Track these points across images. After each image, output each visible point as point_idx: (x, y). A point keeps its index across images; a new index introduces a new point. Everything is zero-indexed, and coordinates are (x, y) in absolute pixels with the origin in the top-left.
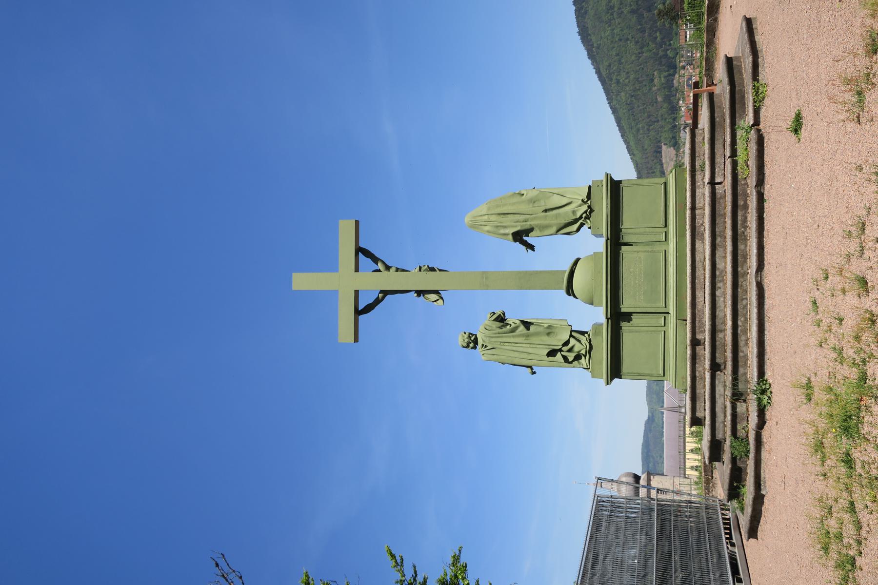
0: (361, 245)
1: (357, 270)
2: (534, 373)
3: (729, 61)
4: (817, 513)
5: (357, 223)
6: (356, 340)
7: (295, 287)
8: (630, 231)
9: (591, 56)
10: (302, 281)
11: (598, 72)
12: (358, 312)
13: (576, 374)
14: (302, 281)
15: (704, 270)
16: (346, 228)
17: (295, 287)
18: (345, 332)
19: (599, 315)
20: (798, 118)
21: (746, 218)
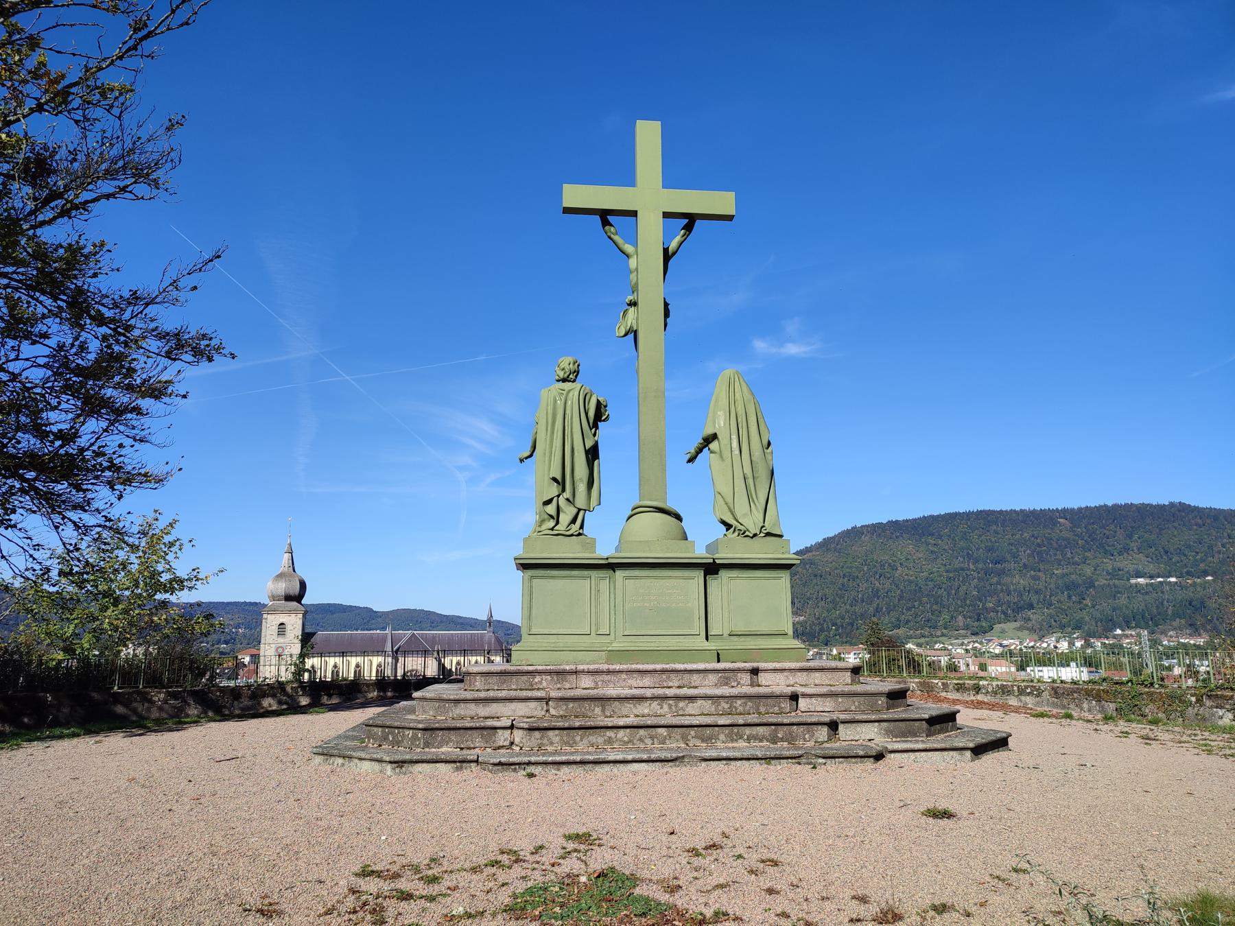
0: (698, 223)
1: (666, 215)
2: (521, 461)
3: (950, 718)
4: (421, 859)
5: (729, 218)
6: (567, 211)
7: (640, 124)
8: (725, 588)
10: (648, 137)
12: (605, 215)
13: (529, 517)
14: (648, 137)
15: (679, 687)
16: (722, 202)
17: (640, 124)
18: (576, 195)
19: (605, 550)
20: (947, 814)
21: (761, 741)
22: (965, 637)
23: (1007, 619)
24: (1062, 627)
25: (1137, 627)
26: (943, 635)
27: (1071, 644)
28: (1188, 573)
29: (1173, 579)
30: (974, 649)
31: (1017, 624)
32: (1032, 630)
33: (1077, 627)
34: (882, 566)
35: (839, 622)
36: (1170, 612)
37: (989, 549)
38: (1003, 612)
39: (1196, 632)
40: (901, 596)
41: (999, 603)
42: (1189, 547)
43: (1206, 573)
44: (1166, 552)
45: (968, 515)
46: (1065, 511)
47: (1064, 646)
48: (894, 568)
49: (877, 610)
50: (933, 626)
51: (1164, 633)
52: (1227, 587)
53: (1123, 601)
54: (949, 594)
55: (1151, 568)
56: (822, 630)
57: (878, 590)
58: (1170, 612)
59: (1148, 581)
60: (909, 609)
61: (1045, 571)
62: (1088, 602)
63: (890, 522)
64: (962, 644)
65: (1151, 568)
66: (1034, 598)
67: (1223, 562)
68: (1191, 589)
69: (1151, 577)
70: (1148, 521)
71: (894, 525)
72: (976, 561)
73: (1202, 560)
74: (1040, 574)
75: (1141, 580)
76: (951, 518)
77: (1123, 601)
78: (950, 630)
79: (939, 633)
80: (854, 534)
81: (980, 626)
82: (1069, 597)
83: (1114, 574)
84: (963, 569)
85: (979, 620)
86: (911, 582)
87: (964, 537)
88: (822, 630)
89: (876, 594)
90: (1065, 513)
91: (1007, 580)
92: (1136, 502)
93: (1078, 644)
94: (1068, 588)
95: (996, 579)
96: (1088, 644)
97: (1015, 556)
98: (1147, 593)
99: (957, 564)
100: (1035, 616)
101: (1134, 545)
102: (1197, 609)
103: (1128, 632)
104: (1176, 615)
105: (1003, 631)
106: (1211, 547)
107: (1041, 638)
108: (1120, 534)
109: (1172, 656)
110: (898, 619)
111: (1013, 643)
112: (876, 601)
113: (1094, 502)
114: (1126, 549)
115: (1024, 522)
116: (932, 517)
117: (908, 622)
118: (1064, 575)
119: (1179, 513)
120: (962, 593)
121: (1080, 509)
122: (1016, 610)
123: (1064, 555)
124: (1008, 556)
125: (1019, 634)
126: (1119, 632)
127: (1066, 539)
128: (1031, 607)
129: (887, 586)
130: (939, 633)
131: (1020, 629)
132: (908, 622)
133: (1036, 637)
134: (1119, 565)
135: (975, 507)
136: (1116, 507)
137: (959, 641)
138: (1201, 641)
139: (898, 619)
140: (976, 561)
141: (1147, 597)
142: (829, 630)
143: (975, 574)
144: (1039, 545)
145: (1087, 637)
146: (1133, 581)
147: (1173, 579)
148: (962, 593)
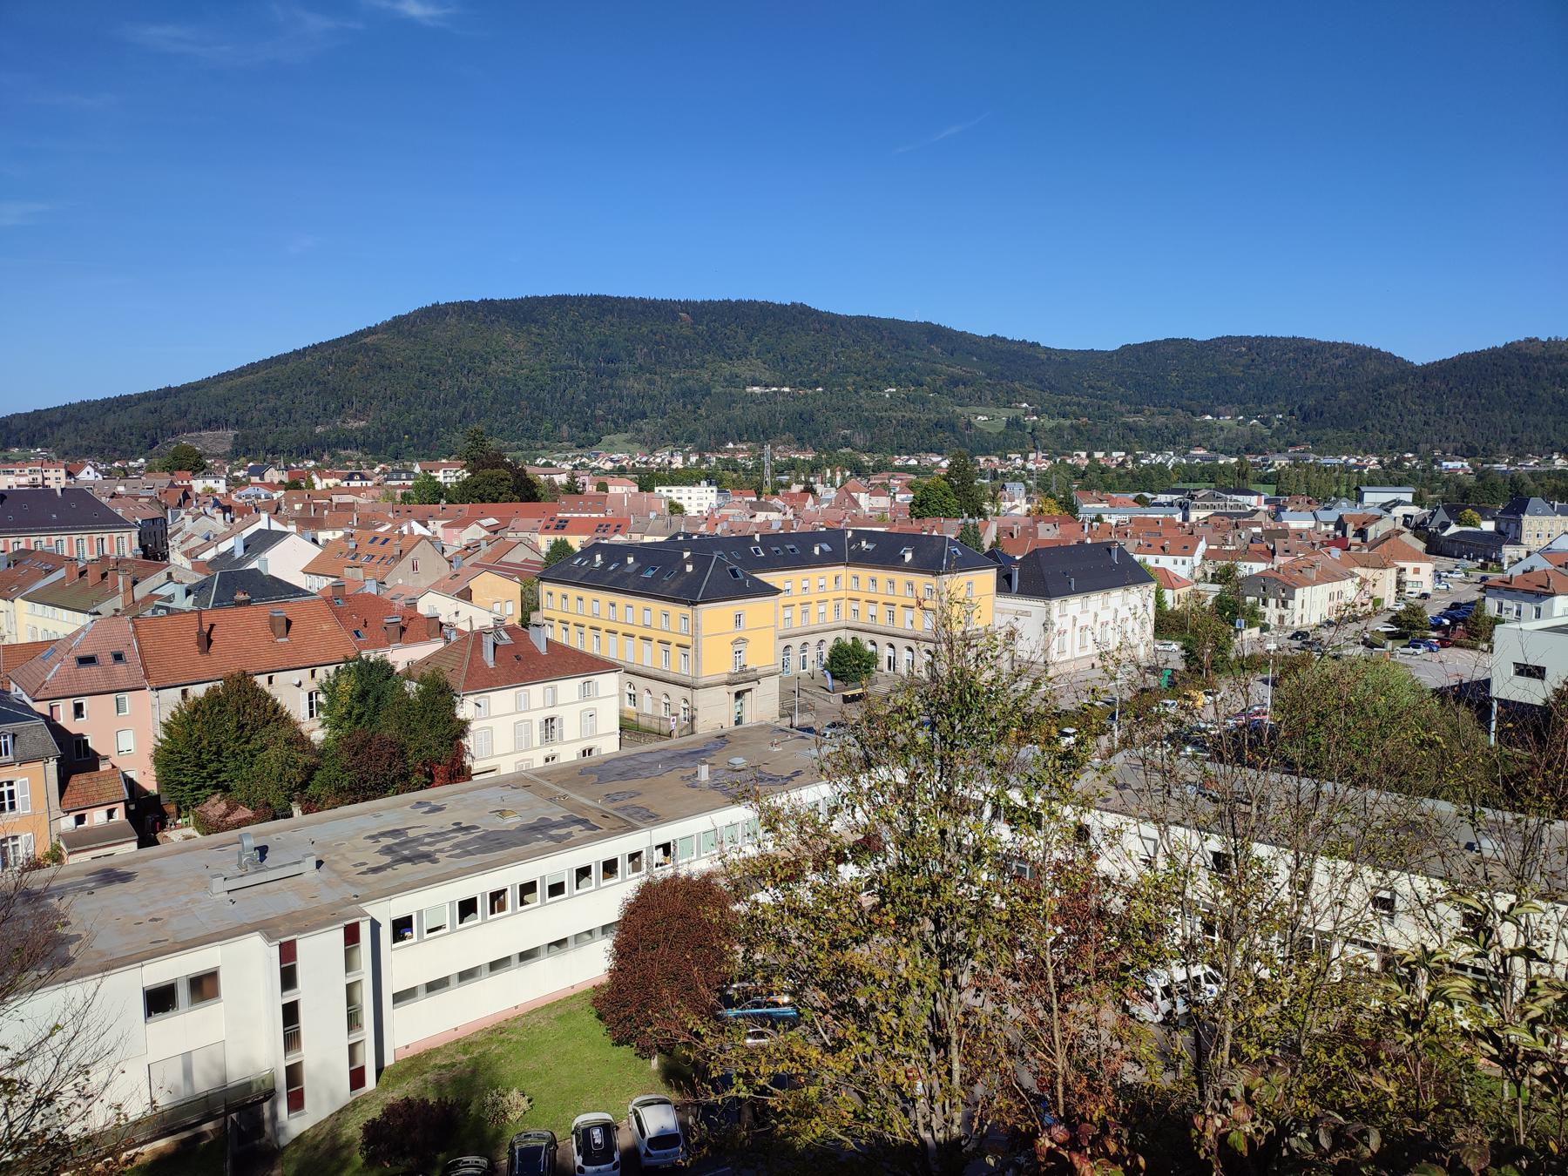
9: (398, 322)
11: (371, 331)
22: (569, 450)
23: (617, 429)
24: (675, 439)
25: (749, 440)
26: (544, 448)
27: (686, 459)
28: (801, 383)
29: (787, 389)
30: (582, 464)
31: (628, 436)
32: (643, 443)
33: (690, 440)
34: (472, 359)
35: (413, 429)
37: (603, 344)
38: (614, 422)
39: (802, 448)
40: (495, 400)
41: (610, 411)
42: (805, 354)
43: (817, 384)
45: (580, 300)
46: (687, 303)
47: (678, 462)
48: (487, 362)
49: (465, 415)
50: (537, 436)
53: (737, 412)
54: (553, 398)
56: (390, 439)
57: (466, 390)
60: (504, 415)
61: (662, 374)
62: (703, 411)
63: (484, 302)
64: (566, 459)
65: (766, 376)
66: (648, 406)
69: (767, 386)
70: (769, 322)
71: (489, 306)
72: (587, 359)
73: (816, 370)
74: (657, 378)
75: (756, 389)
76: (560, 303)
77: (737, 412)
78: (551, 441)
79: (539, 445)
80: (435, 313)
81: (587, 444)
82: (685, 406)
83: (732, 380)
84: (570, 367)
85: (586, 430)
86: (507, 380)
87: (573, 329)
88: (390, 439)
89: (463, 394)
90: (687, 306)
91: (620, 382)
92: (760, 299)
93: (693, 459)
94: (684, 395)
95: (607, 382)
96: (702, 460)
97: (631, 355)
99: (564, 361)
100: (647, 426)
101: (753, 350)
102: (806, 422)
104: (787, 428)
105: (612, 444)
106: (824, 355)
107: (652, 452)
108: (741, 334)
109: (781, 473)
110: (490, 428)
111: (624, 459)
112: (463, 404)
113: (717, 297)
114: (745, 353)
115: (643, 313)
116: (536, 298)
117: (502, 430)
118: (681, 380)
119: (799, 315)
120: (568, 396)
121: (703, 302)
122: (627, 419)
123: (682, 355)
124: (623, 354)
125: (629, 446)
126: (731, 445)
127: (686, 338)
128: (644, 415)
129: (478, 385)
130: (539, 445)
131: (629, 441)
132: (502, 430)
133: (647, 451)
135: (587, 292)
136: (739, 302)
137: (562, 455)
138: (810, 456)
139: (490, 428)
140: (587, 359)
142: (400, 439)
143: (585, 375)
144: (657, 343)
145: (700, 451)
146: (749, 390)
147: (787, 389)
148: (568, 396)
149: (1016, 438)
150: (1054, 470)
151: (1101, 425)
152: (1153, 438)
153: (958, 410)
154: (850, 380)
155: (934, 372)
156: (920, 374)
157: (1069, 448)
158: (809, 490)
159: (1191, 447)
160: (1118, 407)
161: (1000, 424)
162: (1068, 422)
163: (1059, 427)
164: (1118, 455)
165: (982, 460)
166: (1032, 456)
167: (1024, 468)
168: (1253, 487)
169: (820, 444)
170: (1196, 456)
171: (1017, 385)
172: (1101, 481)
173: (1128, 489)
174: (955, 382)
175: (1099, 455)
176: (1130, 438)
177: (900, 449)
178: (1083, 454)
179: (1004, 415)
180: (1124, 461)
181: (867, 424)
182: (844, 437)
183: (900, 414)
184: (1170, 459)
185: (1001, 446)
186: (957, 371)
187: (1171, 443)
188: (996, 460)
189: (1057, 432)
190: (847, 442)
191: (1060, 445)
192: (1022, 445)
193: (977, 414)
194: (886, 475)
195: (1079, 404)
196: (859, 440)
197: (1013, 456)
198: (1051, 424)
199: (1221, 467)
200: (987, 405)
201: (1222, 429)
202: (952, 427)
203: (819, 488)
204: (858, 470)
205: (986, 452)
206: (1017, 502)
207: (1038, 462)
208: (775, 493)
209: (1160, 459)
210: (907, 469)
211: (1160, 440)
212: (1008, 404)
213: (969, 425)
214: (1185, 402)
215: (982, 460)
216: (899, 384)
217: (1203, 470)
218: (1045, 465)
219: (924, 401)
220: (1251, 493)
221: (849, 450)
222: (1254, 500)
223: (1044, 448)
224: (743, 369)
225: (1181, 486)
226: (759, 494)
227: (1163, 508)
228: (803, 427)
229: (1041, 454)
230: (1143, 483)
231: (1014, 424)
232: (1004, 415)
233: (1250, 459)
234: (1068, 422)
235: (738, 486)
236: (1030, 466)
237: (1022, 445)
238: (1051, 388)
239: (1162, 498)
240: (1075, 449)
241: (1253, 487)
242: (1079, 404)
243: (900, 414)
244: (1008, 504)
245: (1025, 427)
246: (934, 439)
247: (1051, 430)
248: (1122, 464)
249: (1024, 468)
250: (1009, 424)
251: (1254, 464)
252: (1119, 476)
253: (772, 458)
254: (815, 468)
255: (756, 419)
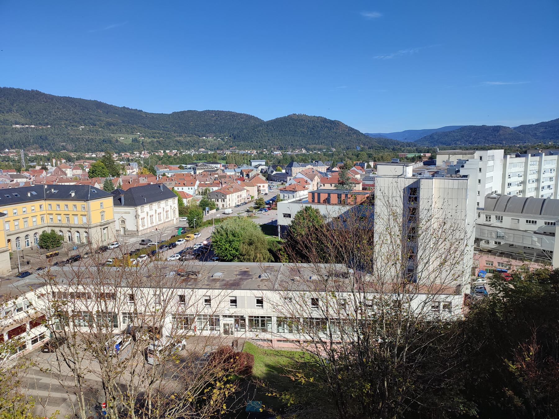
28: (40, 124)
29: (33, 126)
36: (31, 141)
39: (42, 149)
43: (47, 124)
44: (30, 113)
51: (29, 150)
52: (56, 131)
55: (23, 121)
58: (31, 141)
59: (21, 126)
65: (23, 121)
67: (54, 120)
68: (41, 131)
69: (23, 125)
73: (46, 118)
77: (9, 135)
98: (20, 132)
101: (14, 109)
102: (44, 140)
103: (12, 150)
104: (34, 143)
114: (10, 111)
134: (7, 118)
138: (46, 154)
141: (21, 134)
146: (14, 126)
147: (33, 126)
149: (136, 146)
150: (151, 158)
151: (168, 141)
152: (187, 145)
153: (112, 135)
154: (63, 123)
155: (100, 120)
156: (94, 121)
157: (157, 149)
158: (44, 168)
159: (199, 148)
160: (173, 134)
161: (130, 141)
162: (156, 140)
163: (152, 141)
164: (175, 151)
165: (123, 154)
166: (143, 152)
167: (140, 157)
168: (219, 161)
169: (51, 149)
170: (201, 151)
171: (135, 126)
172: (167, 161)
173: (177, 163)
174: (109, 124)
175: (168, 151)
176: (179, 145)
177: (88, 151)
178: (162, 151)
179: (131, 137)
180: (176, 154)
181: (72, 140)
182: (63, 146)
183: (87, 137)
184: (192, 152)
185: (131, 149)
186: (110, 120)
187: (193, 146)
188: (129, 154)
189: (152, 143)
190: (64, 148)
191: (154, 148)
192: (139, 148)
193: (120, 137)
194: (82, 161)
195: (159, 133)
196: (69, 147)
197: (135, 153)
198: (149, 140)
199: (209, 155)
200: (124, 133)
201: (209, 142)
202: (110, 142)
203: (49, 167)
204: (69, 159)
205: (125, 151)
206: (135, 170)
207: (145, 155)
208: (27, 170)
209: (189, 153)
210: (88, 159)
211: (189, 145)
212: (132, 133)
213: (117, 141)
214: (196, 132)
215: (123, 154)
216: (85, 125)
217: (204, 156)
218: (148, 156)
219: (97, 132)
220: (218, 163)
221: (65, 151)
222: (219, 166)
223: (148, 149)
224: (10, 117)
225: (195, 162)
226: (19, 170)
227: (188, 170)
228: (42, 142)
229: (146, 152)
230: (182, 161)
231: (135, 140)
232: (131, 137)
233: (218, 152)
234: (156, 140)
235: (8, 168)
236: (142, 156)
237: (139, 148)
238: (148, 127)
239: (189, 166)
240: (159, 149)
241: (219, 161)
242: (159, 133)
243: (87, 137)
244: (131, 171)
245: (139, 142)
246: (103, 147)
247: (150, 143)
248: (176, 155)
249: (140, 157)
250: (133, 141)
251: (219, 154)
252: (175, 159)
253: (26, 155)
254: (49, 159)
255: (18, 139)
